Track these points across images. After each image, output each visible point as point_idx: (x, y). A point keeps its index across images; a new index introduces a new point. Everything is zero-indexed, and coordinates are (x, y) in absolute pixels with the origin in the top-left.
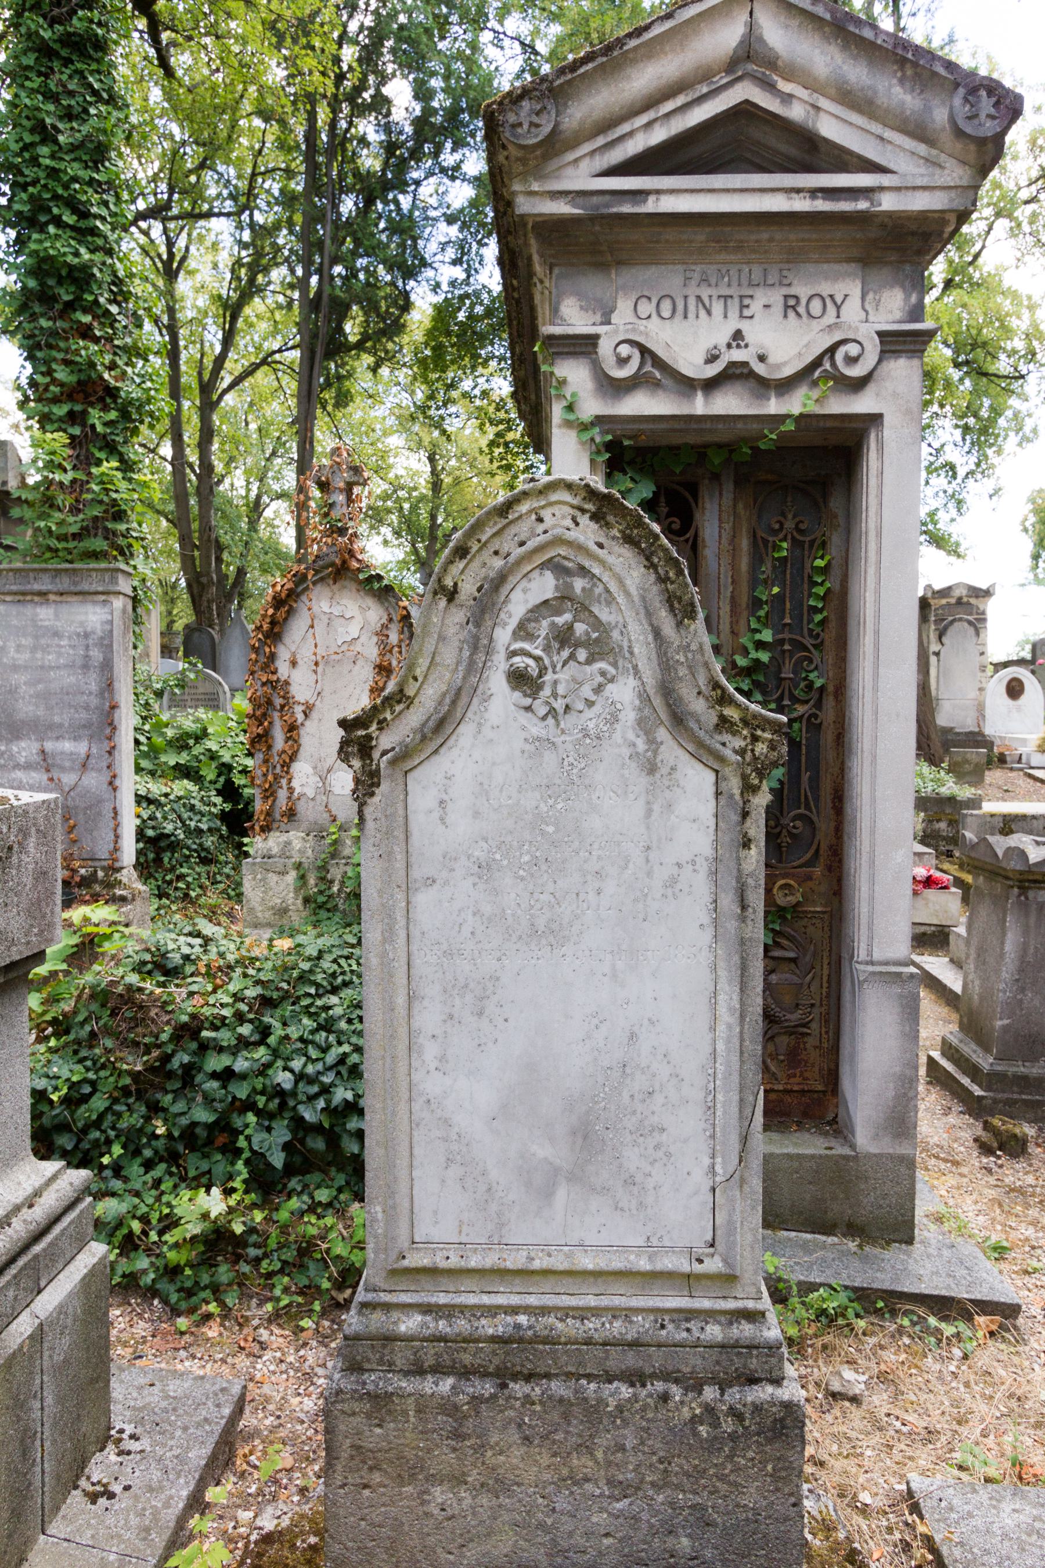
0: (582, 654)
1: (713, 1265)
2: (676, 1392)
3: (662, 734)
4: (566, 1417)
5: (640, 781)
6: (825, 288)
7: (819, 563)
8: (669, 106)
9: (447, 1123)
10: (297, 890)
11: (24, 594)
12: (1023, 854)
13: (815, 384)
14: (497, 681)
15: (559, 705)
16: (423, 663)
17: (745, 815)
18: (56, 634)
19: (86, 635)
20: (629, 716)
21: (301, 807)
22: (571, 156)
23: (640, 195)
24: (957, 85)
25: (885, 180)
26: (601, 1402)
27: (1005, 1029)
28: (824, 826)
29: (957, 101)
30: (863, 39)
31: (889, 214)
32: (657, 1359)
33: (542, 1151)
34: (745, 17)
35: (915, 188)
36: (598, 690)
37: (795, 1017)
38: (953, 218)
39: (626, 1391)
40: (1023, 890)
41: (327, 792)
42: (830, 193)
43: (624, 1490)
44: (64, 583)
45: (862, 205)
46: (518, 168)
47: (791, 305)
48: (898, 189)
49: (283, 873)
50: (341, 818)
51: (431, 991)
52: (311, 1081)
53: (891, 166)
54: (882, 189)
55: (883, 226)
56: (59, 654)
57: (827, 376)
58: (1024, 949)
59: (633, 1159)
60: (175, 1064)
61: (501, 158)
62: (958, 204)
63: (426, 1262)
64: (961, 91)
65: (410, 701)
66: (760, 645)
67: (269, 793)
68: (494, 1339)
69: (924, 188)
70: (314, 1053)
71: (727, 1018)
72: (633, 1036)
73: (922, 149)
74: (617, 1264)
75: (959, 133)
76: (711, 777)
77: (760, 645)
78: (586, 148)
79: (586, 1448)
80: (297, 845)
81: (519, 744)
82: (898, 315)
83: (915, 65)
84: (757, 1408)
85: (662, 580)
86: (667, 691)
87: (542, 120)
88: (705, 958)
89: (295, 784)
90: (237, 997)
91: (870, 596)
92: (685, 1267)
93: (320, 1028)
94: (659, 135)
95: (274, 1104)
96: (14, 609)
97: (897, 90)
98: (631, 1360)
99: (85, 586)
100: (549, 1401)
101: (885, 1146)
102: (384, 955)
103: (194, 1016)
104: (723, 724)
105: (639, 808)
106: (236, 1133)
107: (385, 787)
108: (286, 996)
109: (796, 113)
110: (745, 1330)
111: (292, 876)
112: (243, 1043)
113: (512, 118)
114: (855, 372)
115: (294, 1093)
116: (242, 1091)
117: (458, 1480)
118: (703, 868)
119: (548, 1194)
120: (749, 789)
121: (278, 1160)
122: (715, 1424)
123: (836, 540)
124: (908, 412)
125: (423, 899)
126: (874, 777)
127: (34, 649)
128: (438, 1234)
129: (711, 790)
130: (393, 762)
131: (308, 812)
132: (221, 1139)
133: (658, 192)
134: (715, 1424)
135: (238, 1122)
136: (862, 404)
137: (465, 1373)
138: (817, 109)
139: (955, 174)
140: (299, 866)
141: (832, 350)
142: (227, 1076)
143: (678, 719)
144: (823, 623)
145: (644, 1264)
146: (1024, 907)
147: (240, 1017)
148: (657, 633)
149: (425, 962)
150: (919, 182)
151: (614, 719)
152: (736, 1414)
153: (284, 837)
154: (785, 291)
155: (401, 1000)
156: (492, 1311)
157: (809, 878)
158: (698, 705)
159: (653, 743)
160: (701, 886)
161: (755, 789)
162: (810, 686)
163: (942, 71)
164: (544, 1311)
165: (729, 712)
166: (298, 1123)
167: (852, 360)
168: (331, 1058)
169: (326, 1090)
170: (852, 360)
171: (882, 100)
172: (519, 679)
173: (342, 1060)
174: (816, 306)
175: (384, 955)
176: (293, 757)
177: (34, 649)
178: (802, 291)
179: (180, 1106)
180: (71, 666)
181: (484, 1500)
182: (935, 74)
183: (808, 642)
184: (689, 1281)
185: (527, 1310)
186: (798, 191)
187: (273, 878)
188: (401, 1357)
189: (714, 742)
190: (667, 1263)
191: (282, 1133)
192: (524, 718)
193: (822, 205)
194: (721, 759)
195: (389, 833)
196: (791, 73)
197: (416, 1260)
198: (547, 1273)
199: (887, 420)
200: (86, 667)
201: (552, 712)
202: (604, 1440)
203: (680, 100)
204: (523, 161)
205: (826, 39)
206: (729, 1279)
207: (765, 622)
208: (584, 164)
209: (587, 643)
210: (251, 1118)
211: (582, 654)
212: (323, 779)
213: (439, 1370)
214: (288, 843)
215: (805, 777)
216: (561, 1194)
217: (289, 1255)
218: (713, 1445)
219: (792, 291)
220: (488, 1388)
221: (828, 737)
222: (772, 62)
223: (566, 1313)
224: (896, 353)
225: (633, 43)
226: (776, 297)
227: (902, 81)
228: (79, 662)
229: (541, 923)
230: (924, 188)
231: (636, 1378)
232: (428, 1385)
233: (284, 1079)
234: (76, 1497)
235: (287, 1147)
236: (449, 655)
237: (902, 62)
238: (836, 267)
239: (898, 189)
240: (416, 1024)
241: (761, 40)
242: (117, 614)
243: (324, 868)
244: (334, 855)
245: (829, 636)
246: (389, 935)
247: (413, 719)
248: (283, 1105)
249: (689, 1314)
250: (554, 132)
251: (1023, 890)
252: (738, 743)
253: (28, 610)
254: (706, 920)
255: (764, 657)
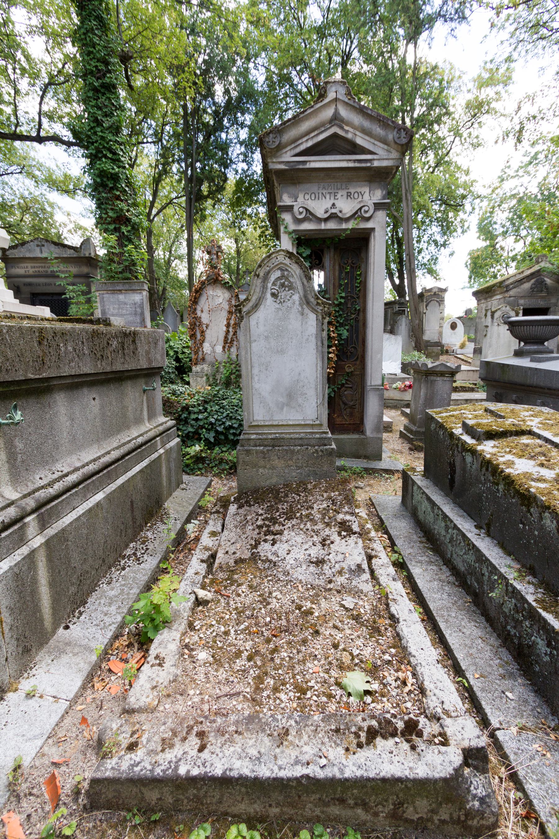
0: (287, 289)
1: (318, 422)
2: (310, 448)
3: (305, 306)
4: (287, 453)
5: (300, 317)
6: (359, 190)
7: (358, 273)
8: (313, 134)
9: (260, 394)
10: (207, 382)
11: (114, 290)
12: (426, 365)
13: (356, 219)
14: (268, 296)
15: (282, 300)
16: (252, 291)
17: (323, 324)
18: (125, 304)
19: (135, 304)
20: (297, 303)
21: (206, 357)
22: (284, 150)
23: (304, 162)
24: (395, 128)
25: (375, 157)
26: (294, 450)
27: (420, 418)
28: (360, 350)
29: (395, 133)
30: (368, 114)
31: (377, 167)
32: (306, 442)
33: (281, 399)
34: (334, 107)
35: (384, 159)
36: (291, 297)
37: (352, 403)
38: (395, 168)
39: (299, 448)
40: (427, 376)
41: (214, 352)
42: (360, 161)
43: (299, 468)
44: (127, 287)
45: (369, 165)
46: (269, 154)
47: (349, 195)
48: (379, 160)
49: (202, 377)
50: (219, 360)
51: (256, 365)
52: (219, 421)
53: (377, 152)
54: (374, 159)
55: (375, 170)
56: (127, 310)
57: (359, 217)
58: (426, 394)
59: (300, 400)
60: (183, 416)
61: (264, 152)
62: (396, 164)
63: (256, 424)
64: (396, 130)
65: (249, 300)
66: (342, 297)
67: (196, 353)
68: (271, 439)
69: (386, 159)
70: (219, 414)
71: (319, 369)
72: (300, 374)
73: (386, 147)
74: (297, 423)
75: (396, 143)
76: (315, 316)
77: (342, 297)
78: (289, 148)
79: (291, 459)
80: (206, 369)
81: (273, 309)
82: (380, 198)
83: (383, 121)
84: (326, 450)
85: (304, 272)
86: (305, 296)
87: (276, 140)
88: (315, 356)
89: (204, 350)
90: (197, 400)
91: (371, 282)
92: (311, 423)
93: (221, 408)
94: (310, 144)
95: (210, 427)
96: (111, 296)
97: (378, 129)
98: (300, 442)
99: (134, 288)
100: (283, 450)
101: (375, 435)
102: (245, 358)
103: (187, 405)
104: (318, 304)
105: (300, 323)
106: (200, 434)
107: (245, 319)
108: (211, 400)
109: (349, 136)
110: (324, 435)
111: (205, 378)
112: (200, 412)
113: (267, 140)
114: (367, 215)
115: (215, 424)
116: (201, 423)
117: (265, 467)
118: (314, 336)
119: (282, 409)
120: (323, 318)
121: (212, 440)
122: (318, 453)
123: (363, 266)
124: (382, 227)
125: (254, 345)
126: (372, 334)
127: (119, 309)
128: (259, 418)
129: (315, 319)
130: (246, 314)
131: (209, 358)
132: (196, 437)
133: (310, 161)
134: (318, 453)
135: (200, 431)
136: (369, 225)
137: (266, 446)
138: (356, 135)
139: (395, 155)
140: (207, 375)
141: (360, 209)
142: (197, 420)
143: (308, 303)
144: (359, 291)
145: (303, 423)
146: (427, 382)
147: (199, 405)
148: (303, 284)
149: (255, 359)
150: (385, 157)
151: (294, 303)
152: (322, 451)
153: (202, 366)
154: (347, 191)
155: (249, 367)
156: (271, 434)
157: (355, 364)
158: (312, 300)
159: (302, 308)
160: (313, 340)
161: (325, 318)
162: (356, 309)
163: (391, 123)
164: (282, 433)
165: (319, 301)
166: (217, 432)
167: (366, 212)
168: (225, 415)
169: (224, 423)
170: (366, 212)
171: (374, 132)
172: (273, 295)
173: (228, 415)
174: (356, 195)
175: (245, 358)
176: (203, 341)
177: (119, 309)
178: (352, 191)
179: (184, 428)
180: (131, 314)
181: (270, 471)
182: (389, 124)
183: (355, 296)
184: (312, 426)
185: (278, 433)
186: (350, 160)
187: (199, 379)
188: (252, 443)
189: (316, 308)
190: (308, 422)
191: (212, 434)
192: (274, 304)
193: (357, 165)
194: (317, 312)
195: (246, 330)
196: (348, 124)
197: (254, 424)
198: (282, 425)
199: (376, 229)
200: (136, 314)
201: (281, 302)
202: (295, 458)
203: (316, 133)
204: (271, 152)
205: (358, 113)
206: (321, 425)
207: (343, 291)
208: (288, 153)
209: (288, 286)
210: (204, 430)
211: (287, 289)
212: (213, 348)
213: (260, 446)
214: (203, 368)
215: (354, 336)
216: (285, 409)
217: (217, 462)
218: (317, 458)
219: (349, 191)
220: (270, 448)
221: (361, 324)
222: (342, 120)
223: (286, 433)
224: (379, 209)
225: (302, 115)
226: (344, 193)
227: (379, 126)
228: (133, 313)
229: (279, 349)
230: (386, 159)
231: (301, 445)
232: (258, 448)
233: (213, 420)
234: (178, 490)
235: (214, 437)
236: (258, 290)
237: (380, 121)
238: (362, 183)
239: (379, 160)
240: (253, 372)
241: (339, 114)
242: (144, 297)
243: (214, 375)
244: (217, 372)
245: (361, 295)
246: (246, 353)
247: (251, 304)
248: (212, 427)
249: (312, 433)
250: (280, 144)
251: (427, 376)
252: (321, 308)
253: (116, 296)
254: (315, 347)
255: (343, 301)
